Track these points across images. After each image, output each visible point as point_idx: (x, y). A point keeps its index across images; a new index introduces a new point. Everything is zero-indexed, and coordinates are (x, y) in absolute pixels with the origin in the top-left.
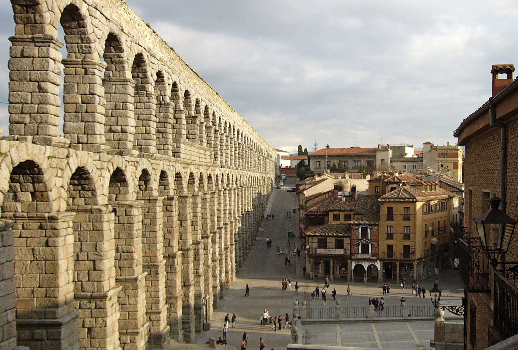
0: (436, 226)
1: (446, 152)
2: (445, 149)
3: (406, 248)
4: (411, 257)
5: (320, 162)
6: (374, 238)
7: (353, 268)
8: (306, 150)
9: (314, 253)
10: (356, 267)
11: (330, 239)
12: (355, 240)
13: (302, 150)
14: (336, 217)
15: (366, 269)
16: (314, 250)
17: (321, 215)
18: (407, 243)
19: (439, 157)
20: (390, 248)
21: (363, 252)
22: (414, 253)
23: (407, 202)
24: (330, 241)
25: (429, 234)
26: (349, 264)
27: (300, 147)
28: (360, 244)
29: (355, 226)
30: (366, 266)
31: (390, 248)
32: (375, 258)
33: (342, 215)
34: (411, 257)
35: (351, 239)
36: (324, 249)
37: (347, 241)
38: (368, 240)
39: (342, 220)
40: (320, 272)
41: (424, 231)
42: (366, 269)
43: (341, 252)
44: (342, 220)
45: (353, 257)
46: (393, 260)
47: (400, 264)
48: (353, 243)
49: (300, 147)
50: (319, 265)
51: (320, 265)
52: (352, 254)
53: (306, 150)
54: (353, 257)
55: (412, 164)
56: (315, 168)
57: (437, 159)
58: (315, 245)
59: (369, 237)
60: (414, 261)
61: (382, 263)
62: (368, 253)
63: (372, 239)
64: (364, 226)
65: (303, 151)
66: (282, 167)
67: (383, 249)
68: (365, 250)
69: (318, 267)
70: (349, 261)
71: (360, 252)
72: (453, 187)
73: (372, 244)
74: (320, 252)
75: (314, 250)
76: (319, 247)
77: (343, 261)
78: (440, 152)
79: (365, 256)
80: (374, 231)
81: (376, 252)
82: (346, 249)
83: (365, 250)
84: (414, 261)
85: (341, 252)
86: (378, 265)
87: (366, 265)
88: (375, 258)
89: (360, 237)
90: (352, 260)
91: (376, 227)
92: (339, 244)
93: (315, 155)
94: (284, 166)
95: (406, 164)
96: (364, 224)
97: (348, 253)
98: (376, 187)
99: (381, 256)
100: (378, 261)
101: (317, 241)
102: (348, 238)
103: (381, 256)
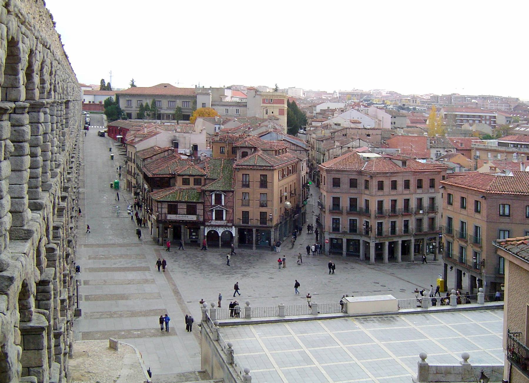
0: (288, 190)
1: (272, 98)
2: (270, 95)
3: (263, 215)
4: (269, 224)
5: (130, 100)
6: (230, 204)
7: (206, 234)
8: (109, 84)
9: (163, 218)
10: (209, 233)
11: (181, 205)
12: (208, 206)
13: (105, 84)
14: (186, 182)
15: (220, 235)
16: (163, 215)
17: (167, 177)
18: (264, 210)
19: (264, 102)
20: (245, 214)
21: (216, 219)
22: (271, 220)
23: (264, 169)
24: (181, 207)
25: (284, 198)
26: (202, 230)
27: (103, 81)
28: (214, 210)
29: (208, 192)
30: (220, 232)
31: (245, 214)
32: (230, 224)
33: (192, 180)
34: (269, 224)
35: (204, 206)
37: (200, 207)
38: (223, 206)
39: (192, 185)
40: (168, 237)
41: (279, 196)
43: (193, 218)
44: (192, 185)
46: (250, 227)
47: (257, 230)
48: (206, 209)
49: (103, 81)
50: (167, 230)
51: (168, 230)
52: (205, 221)
53: (109, 84)
54: (207, 224)
55: (235, 108)
56: (126, 107)
57: (262, 105)
58: (165, 210)
59: (223, 204)
60: (271, 227)
62: (222, 219)
64: (218, 193)
65: (106, 85)
66: (85, 103)
67: (238, 215)
68: (219, 216)
69: (166, 231)
70: (202, 227)
72: (297, 146)
73: (226, 211)
74: (171, 218)
75: (163, 215)
76: (169, 213)
77: (195, 226)
78: (265, 98)
79: (219, 223)
80: (229, 198)
81: (231, 219)
82: (198, 215)
83: (219, 216)
84: (271, 227)
86: (234, 231)
87: (220, 231)
88: (230, 224)
89: (213, 203)
90: (205, 226)
91: (231, 194)
92: (191, 210)
93: (126, 94)
94: (87, 102)
95: (227, 108)
97: (201, 219)
98: (221, 147)
99: (236, 222)
100: (234, 227)
101: (166, 206)
102: (201, 204)
103: (236, 222)
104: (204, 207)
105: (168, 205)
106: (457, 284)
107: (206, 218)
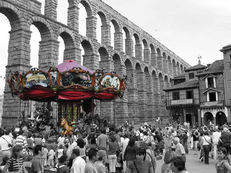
7: (202, 116)
11: (182, 92)
12: (202, 90)
26: (199, 113)
32: (221, 105)
35: (199, 90)
36: (177, 100)
37: (196, 92)
38: (214, 88)
42: (214, 116)
43: (190, 101)
45: (202, 106)
59: (215, 86)
61: (230, 109)
63: (219, 87)
68: (213, 98)
70: (199, 110)
71: (208, 100)
73: (218, 92)
77: (193, 109)
83: (213, 98)
85: (190, 101)
87: (214, 113)
89: (207, 87)
96: (209, 74)
100: (226, 108)
104: (199, 92)
105: (173, 93)
106: (188, 95)
107: (202, 101)
